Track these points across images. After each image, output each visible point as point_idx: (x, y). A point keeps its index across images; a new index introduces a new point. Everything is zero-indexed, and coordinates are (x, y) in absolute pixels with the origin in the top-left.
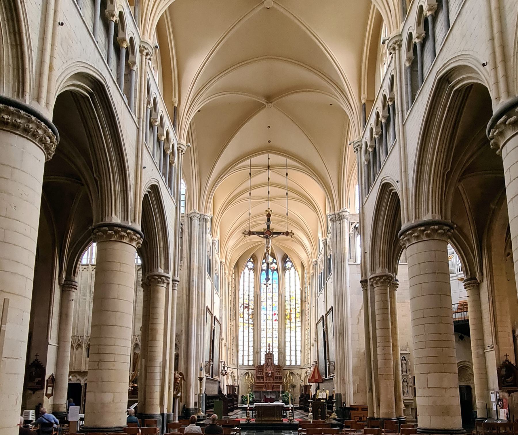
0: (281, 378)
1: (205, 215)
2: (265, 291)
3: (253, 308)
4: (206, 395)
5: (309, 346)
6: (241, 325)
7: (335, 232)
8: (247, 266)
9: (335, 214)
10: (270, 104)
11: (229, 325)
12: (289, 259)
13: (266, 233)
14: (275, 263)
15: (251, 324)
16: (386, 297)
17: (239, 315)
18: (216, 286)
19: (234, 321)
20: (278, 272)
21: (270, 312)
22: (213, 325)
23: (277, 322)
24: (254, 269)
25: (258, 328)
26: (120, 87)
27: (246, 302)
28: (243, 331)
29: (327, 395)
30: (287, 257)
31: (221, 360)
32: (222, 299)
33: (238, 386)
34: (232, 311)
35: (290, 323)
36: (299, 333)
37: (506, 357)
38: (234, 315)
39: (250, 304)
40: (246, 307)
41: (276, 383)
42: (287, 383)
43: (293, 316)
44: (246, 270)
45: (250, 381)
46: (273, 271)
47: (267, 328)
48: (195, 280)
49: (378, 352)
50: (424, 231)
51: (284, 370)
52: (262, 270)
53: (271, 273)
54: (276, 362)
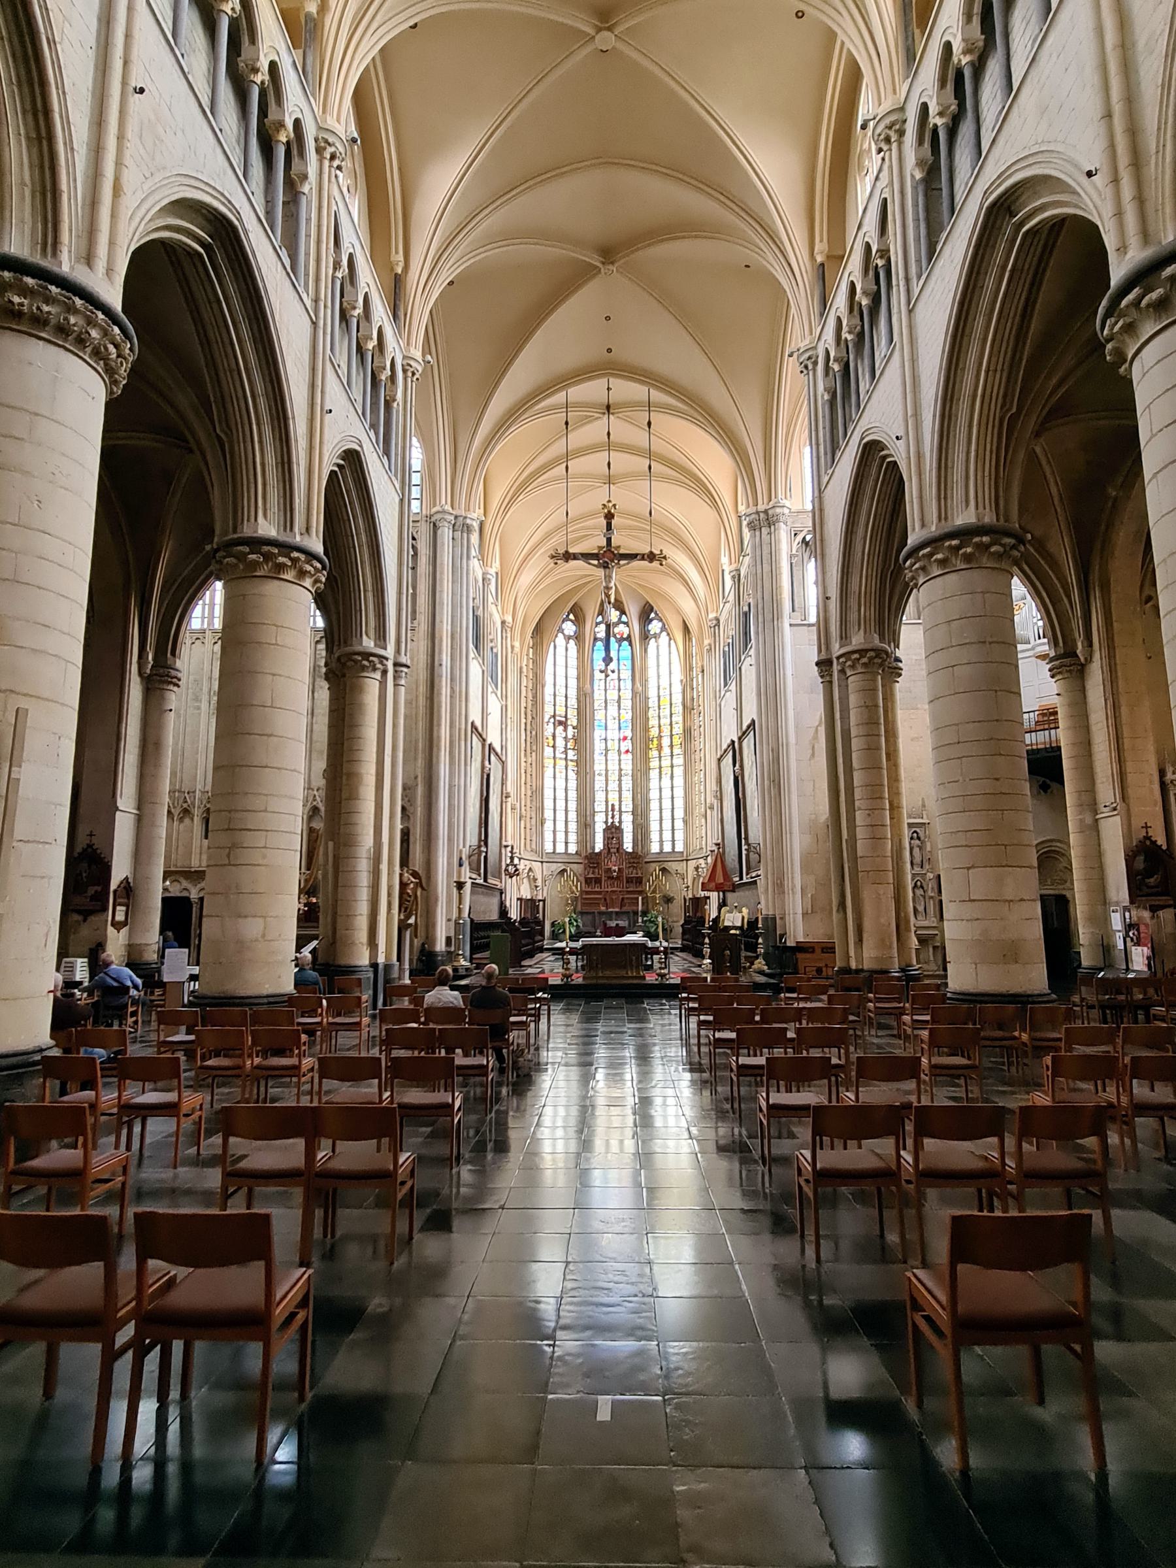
0: (639, 881)
1: (465, 518)
2: (603, 687)
3: (575, 724)
4: (472, 921)
5: (703, 810)
6: (548, 763)
7: (758, 553)
9: (758, 513)
10: (611, 267)
11: (523, 764)
12: (656, 614)
13: (603, 555)
14: (624, 623)
15: (572, 761)
16: (875, 698)
17: (545, 740)
18: (492, 676)
19: (534, 754)
20: (630, 644)
21: (613, 734)
22: (487, 763)
23: (630, 756)
24: (578, 637)
25: (588, 771)
27: (561, 711)
28: (555, 778)
29: (743, 918)
30: (652, 609)
31: (504, 843)
32: (506, 706)
33: (544, 901)
34: (528, 733)
35: (660, 757)
36: (679, 781)
37: (1144, 830)
38: (534, 741)
39: (569, 716)
40: (560, 723)
41: (629, 892)
42: (654, 892)
43: (666, 742)
44: (560, 640)
45: (571, 888)
46: (620, 641)
47: (607, 770)
48: (444, 663)
49: (858, 822)
50: (958, 548)
52: (596, 639)
53: (617, 645)
54: (628, 846)
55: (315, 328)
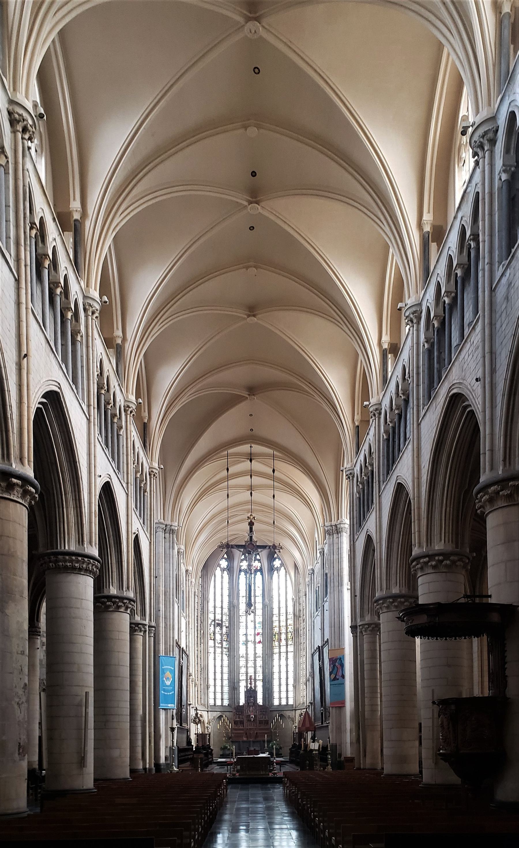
0: (267, 722)
1: (171, 526)
3: (227, 625)
6: (211, 650)
8: (219, 565)
10: (253, 397)
15: (225, 648)
16: (376, 646)
18: (182, 608)
19: (202, 645)
20: (262, 574)
21: (251, 631)
24: (230, 569)
25: (235, 655)
26: (45, 330)
27: (218, 617)
34: (199, 632)
35: (280, 646)
39: (224, 620)
40: (218, 625)
43: (283, 637)
44: (218, 572)
51: (271, 711)
54: (260, 701)
55: (127, 497)
